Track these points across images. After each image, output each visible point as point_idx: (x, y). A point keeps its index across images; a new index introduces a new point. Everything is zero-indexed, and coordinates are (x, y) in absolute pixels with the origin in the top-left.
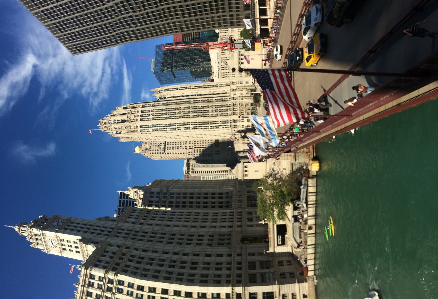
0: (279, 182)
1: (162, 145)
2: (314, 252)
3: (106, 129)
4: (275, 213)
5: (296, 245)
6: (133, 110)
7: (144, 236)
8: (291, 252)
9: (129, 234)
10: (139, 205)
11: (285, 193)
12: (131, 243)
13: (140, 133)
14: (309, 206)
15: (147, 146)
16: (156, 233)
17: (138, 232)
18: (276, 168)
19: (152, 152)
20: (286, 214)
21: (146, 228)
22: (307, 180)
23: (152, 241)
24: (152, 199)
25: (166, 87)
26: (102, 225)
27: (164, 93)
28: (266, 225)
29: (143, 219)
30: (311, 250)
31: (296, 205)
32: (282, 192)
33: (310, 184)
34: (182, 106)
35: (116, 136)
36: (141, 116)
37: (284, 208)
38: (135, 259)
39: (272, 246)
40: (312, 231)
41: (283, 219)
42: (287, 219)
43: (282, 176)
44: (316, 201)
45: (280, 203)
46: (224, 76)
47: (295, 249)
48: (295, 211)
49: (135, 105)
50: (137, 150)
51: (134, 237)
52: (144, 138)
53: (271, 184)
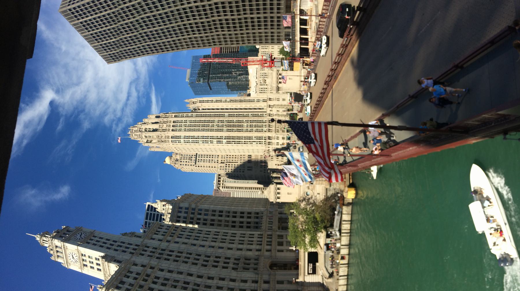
0: (312, 206)
1: (193, 157)
2: (346, 283)
3: (136, 137)
4: (307, 240)
5: (328, 275)
6: (165, 120)
7: (171, 255)
8: (322, 282)
9: (154, 252)
10: (167, 221)
11: (318, 219)
12: (156, 263)
13: (171, 144)
14: (342, 235)
15: (178, 157)
16: (182, 253)
17: (164, 250)
18: (310, 192)
19: (182, 163)
20: (318, 242)
22: (341, 207)
23: (177, 261)
24: (179, 214)
25: (201, 99)
26: (127, 242)
27: (198, 105)
28: (297, 252)
29: (170, 236)
30: (343, 281)
31: (329, 233)
32: (315, 218)
33: (344, 212)
34: (216, 119)
35: (146, 145)
36: (173, 126)
37: (316, 234)
38: (160, 281)
39: (302, 275)
40: (345, 261)
41: (314, 246)
42: (319, 248)
43: (315, 201)
44: (350, 230)
45: (313, 230)
46: (262, 91)
47: (326, 280)
48: (327, 239)
49: (168, 115)
50: (168, 161)
52: (175, 149)
53: (304, 209)
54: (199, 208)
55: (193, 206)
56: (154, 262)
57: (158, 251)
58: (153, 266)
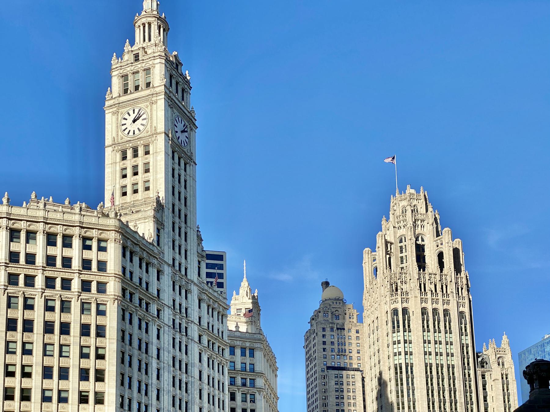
6: (452, 288)
12: (166, 321)
13: (389, 308)
21: (195, 349)
24: (238, 352)
26: (189, 248)
29: (209, 341)
35: (380, 243)
36: (435, 311)
51: (177, 326)
56: (167, 315)
57: (184, 321)
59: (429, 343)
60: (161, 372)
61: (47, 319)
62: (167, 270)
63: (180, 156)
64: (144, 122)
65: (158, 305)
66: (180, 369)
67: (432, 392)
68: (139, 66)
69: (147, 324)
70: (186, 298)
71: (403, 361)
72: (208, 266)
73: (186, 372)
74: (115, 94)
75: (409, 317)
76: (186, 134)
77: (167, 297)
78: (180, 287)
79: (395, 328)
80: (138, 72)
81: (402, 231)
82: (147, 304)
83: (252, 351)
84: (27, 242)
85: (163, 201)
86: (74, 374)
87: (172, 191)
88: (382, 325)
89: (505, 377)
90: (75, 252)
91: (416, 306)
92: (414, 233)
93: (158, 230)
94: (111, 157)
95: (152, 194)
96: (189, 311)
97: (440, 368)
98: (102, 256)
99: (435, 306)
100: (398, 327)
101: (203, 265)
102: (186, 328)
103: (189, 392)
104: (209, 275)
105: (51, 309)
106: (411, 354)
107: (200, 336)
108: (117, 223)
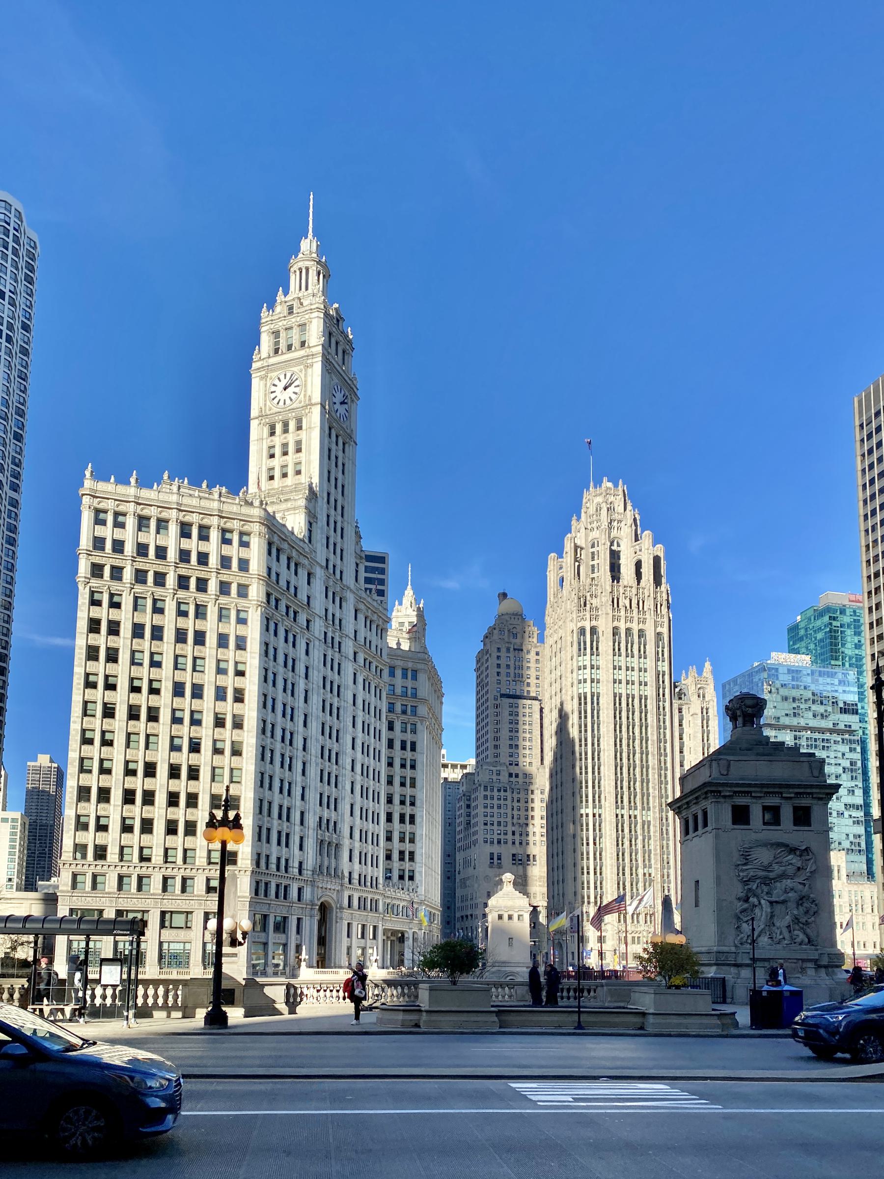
6: (649, 604)
12: (317, 634)
21: (349, 668)
24: (399, 673)
26: (345, 547)
35: (568, 547)
36: (628, 630)
49: (664, 610)
51: (329, 640)
54: (419, 725)
55: (422, 710)
56: (318, 627)
57: (337, 634)
58: (311, 623)
59: (620, 669)
60: (310, 693)
61: (179, 626)
62: (319, 573)
63: (338, 435)
64: (297, 390)
65: (308, 614)
66: (331, 692)
67: (620, 727)
68: (293, 320)
69: (294, 636)
70: (341, 607)
71: (588, 690)
72: (367, 570)
73: (338, 695)
74: (264, 354)
75: (598, 638)
76: (346, 406)
77: (319, 604)
78: (334, 593)
79: (581, 651)
80: (291, 328)
81: (595, 534)
82: (295, 613)
83: (415, 673)
84: (158, 532)
85: (316, 489)
86: (209, 693)
87: (327, 475)
88: (566, 646)
89: (705, 711)
90: (213, 547)
91: (606, 624)
92: (609, 537)
93: (310, 524)
94: (257, 431)
95: (303, 479)
96: (343, 622)
97: (630, 700)
98: (244, 553)
99: (629, 625)
100: (585, 649)
101: (362, 568)
102: (340, 643)
103: (341, 718)
104: (368, 580)
105: (184, 614)
106: (598, 682)
107: (355, 653)
108: (262, 513)
